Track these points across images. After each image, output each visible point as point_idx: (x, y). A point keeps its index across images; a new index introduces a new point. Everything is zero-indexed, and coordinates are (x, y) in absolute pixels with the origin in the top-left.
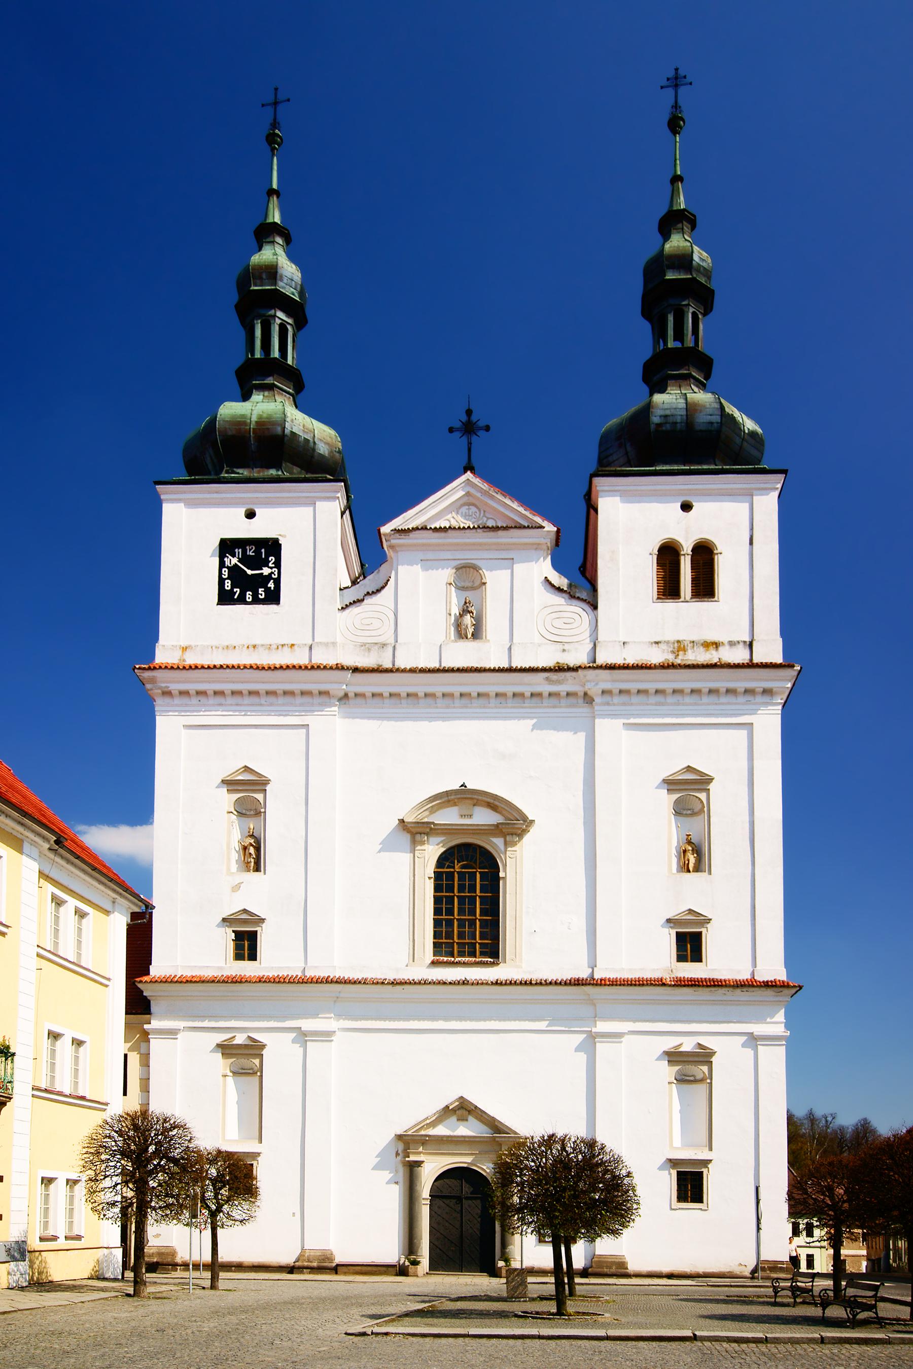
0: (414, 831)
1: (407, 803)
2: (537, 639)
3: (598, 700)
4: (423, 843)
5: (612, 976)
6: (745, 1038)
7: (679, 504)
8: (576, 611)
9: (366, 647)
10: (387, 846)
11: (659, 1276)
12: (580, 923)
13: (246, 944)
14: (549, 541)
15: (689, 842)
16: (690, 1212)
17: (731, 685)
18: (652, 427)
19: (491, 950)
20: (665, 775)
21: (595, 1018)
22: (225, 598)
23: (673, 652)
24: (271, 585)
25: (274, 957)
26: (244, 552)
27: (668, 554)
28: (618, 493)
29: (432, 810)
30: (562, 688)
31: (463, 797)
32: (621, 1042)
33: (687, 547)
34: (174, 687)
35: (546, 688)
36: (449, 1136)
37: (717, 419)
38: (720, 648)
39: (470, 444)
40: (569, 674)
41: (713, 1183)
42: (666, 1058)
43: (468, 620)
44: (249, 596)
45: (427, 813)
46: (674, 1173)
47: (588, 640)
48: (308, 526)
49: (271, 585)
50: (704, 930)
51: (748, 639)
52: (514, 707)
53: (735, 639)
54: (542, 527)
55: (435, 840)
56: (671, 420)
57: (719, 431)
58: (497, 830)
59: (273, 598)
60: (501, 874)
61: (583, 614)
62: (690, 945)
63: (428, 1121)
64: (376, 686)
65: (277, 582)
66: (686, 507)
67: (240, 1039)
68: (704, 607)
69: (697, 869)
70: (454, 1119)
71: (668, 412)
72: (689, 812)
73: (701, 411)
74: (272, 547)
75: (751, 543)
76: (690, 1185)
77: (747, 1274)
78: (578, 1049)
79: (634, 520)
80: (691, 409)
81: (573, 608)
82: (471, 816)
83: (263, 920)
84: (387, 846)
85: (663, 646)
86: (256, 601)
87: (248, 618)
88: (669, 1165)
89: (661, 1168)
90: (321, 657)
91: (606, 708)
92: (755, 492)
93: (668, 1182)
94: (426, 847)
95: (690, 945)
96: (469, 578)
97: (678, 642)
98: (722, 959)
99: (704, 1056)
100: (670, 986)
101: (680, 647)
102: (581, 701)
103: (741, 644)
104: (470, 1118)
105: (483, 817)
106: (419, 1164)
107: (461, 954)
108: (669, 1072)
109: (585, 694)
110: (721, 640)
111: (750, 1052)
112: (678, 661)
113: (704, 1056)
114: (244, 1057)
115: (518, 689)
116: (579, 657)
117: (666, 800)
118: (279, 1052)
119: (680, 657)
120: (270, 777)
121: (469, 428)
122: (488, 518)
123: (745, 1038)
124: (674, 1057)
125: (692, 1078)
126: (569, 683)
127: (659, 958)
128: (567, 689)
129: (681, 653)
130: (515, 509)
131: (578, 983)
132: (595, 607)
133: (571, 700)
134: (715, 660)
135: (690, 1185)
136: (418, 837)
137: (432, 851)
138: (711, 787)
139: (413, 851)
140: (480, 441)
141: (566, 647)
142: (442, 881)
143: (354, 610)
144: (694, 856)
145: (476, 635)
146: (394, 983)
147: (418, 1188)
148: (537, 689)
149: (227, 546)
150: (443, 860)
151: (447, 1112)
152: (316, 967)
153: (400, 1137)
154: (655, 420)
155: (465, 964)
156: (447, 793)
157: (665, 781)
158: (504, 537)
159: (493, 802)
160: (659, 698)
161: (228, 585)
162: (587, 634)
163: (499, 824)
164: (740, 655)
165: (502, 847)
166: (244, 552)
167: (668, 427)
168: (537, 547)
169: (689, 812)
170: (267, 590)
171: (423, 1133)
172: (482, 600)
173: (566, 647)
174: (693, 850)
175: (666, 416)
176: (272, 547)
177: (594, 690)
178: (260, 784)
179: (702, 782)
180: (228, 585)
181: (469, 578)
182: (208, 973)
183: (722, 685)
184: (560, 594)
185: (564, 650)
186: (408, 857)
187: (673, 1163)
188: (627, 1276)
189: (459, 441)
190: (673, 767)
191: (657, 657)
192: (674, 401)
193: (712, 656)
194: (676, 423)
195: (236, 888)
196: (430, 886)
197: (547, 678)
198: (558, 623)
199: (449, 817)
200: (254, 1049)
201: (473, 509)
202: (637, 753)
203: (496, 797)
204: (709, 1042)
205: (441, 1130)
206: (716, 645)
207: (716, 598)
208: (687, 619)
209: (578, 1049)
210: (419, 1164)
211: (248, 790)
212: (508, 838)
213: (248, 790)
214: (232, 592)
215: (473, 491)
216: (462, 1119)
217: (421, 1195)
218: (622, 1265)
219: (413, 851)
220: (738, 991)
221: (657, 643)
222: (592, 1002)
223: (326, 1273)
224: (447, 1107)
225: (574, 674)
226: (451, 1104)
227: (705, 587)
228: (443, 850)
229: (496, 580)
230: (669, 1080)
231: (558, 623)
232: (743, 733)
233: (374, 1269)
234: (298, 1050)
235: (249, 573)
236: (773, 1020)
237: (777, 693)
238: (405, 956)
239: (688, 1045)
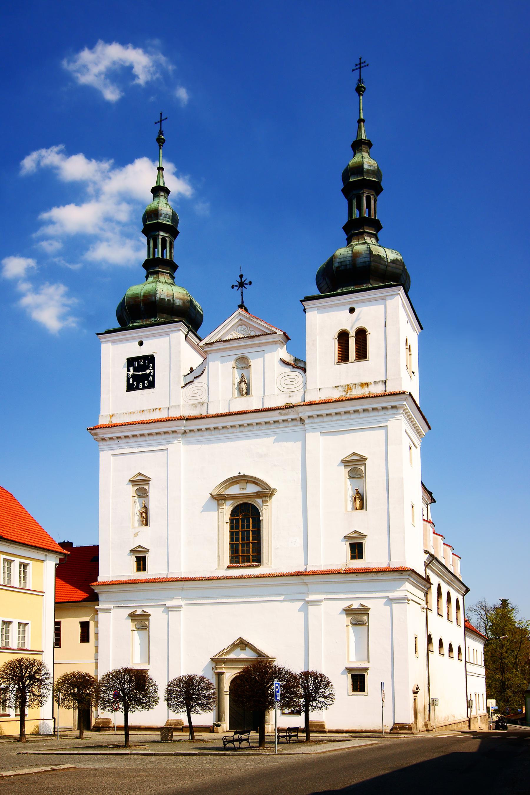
0: (219, 499)
2: (277, 392)
3: (307, 421)
4: (223, 505)
5: (315, 569)
6: (385, 600)
7: (348, 311)
8: (297, 374)
9: (195, 405)
10: (206, 508)
11: (342, 732)
12: (300, 541)
13: (141, 563)
14: (281, 339)
15: (358, 493)
16: (359, 696)
17: (374, 406)
18: (334, 269)
19: (257, 559)
20: (342, 458)
21: (308, 593)
22: (130, 388)
23: (345, 391)
24: (151, 379)
25: (154, 569)
26: (138, 363)
27: (343, 336)
28: (316, 308)
29: (226, 488)
30: (289, 417)
31: (241, 479)
32: (321, 605)
33: (352, 333)
34: (106, 436)
35: (281, 418)
36: (236, 658)
37: (367, 259)
38: (370, 386)
39: (242, 292)
40: (290, 410)
41: (370, 680)
42: (345, 612)
43: (243, 385)
44: (141, 386)
45: (223, 489)
46: (350, 676)
47: (302, 390)
48: (169, 346)
49: (151, 379)
50: (363, 541)
51: (384, 380)
52: (266, 429)
53: (377, 380)
54: (276, 333)
55: (229, 502)
56: (344, 264)
57: (369, 266)
58: (258, 495)
59: (152, 385)
60: (261, 518)
61: (300, 376)
62: (357, 550)
63: (225, 651)
64: (199, 425)
65: (153, 377)
66: (352, 310)
67: (139, 612)
68: (362, 364)
69: (362, 507)
70: (239, 649)
71: (342, 260)
72: (358, 476)
73: (359, 256)
74: (150, 359)
75: (385, 326)
76: (358, 682)
77: (388, 731)
78: (300, 610)
79: (325, 321)
80: (355, 255)
82: (245, 489)
83: (148, 550)
84: (206, 508)
85: (339, 388)
86: (144, 388)
87: (141, 396)
88: (347, 671)
89: (342, 673)
90: (174, 414)
91: (311, 425)
92: (387, 298)
93: (347, 680)
94: (224, 507)
95: (357, 550)
96: (243, 363)
97: (348, 385)
99: (365, 611)
100: (343, 573)
101: (348, 388)
102: (299, 422)
103: (381, 382)
104: (247, 648)
105: (252, 489)
106: (222, 673)
107: (243, 562)
108: (346, 620)
109: (301, 419)
110: (370, 381)
111: (389, 608)
112: (348, 396)
113: (365, 611)
114: (141, 621)
115: (267, 420)
116: (296, 399)
117: (344, 472)
118: (157, 617)
119: (348, 393)
121: (241, 285)
122: (251, 331)
123: (385, 600)
124: (348, 611)
125: (361, 623)
126: (291, 415)
128: (290, 417)
129: (349, 391)
130: (263, 325)
131: (298, 574)
132: (305, 370)
133: (294, 423)
134: (367, 394)
135: (358, 682)
136: (220, 502)
137: (227, 509)
138: (366, 462)
139: (218, 510)
140: (247, 291)
142: (234, 524)
143: (189, 387)
145: (248, 393)
146: (208, 579)
147: (222, 686)
148: (276, 419)
149: (130, 362)
150: (234, 513)
151: (234, 646)
152: (172, 573)
153: (212, 659)
154: (336, 265)
155: (244, 567)
156: (232, 478)
157: (342, 461)
158: (257, 341)
159: (255, 481)
160: (338, 417)
161: (131, 381)
162: (302, 386)
163: (257, 492)
164: (379, 389)
165: (261, 503)
166: (138, 363)
167: (343, 268)
168: (276, 342)
169: (358, 476)
170: (149, 382)
171: (224, 657)
172: (249, 374)
173: (291, 394)
174: (359, 497)
175: (341, 262)
176: (150, 359)
177: (304, 415)
178: (147, 481)
179: (362, 460)
180: (131, 381)
181: (243, 363)
182: (124, 579)
183: (370, 407)
184: (288, 366)
185: (290, 396)
186: (216, 513)
187: (349, 670)
188: (325, 732)
189: (236, 292)
190: (345, 454)
191: (336, 395)
192: (346, 253)
193: (365, 391)
194: (347, 265)
195: (136, 535)
196: (227, 528)
197: (280, 413)
198: (287, 382)
199: (235, 490)
200: (146, 616)
201: (244, 327)
202: (327, 448)
203: (255, 478)
204: (366, 603)
205: (232, 656)
206: (367, 384)
207: (367, 359)
208: (354, 372)
209: (300, 610)
210: (222, 673)
211: (141, 485)
212: (264, 499)
213: (141, 485)
214: (133, 384)
215: (242, 318)
216: (243, 649)
217: (223, 690)
218: (322, 726)
219: (218, 510)
220: (379, 574)
221: (336, 387)
222: (306, 584)
223: (178, 731)
224: (234, 643)
225: (292, 409)
226: (236, 641)
227: (362, 354)
228: (232, 508)
229: (256, 363)
230: (346, 624)
231: (287, 382)
232: (383, 432)
233: (200, 729)
234: (165, 616)
235: (141, 373)
236: (401, 589)
237: (399, 408)
238: (215, 565)
239: (356, 605)
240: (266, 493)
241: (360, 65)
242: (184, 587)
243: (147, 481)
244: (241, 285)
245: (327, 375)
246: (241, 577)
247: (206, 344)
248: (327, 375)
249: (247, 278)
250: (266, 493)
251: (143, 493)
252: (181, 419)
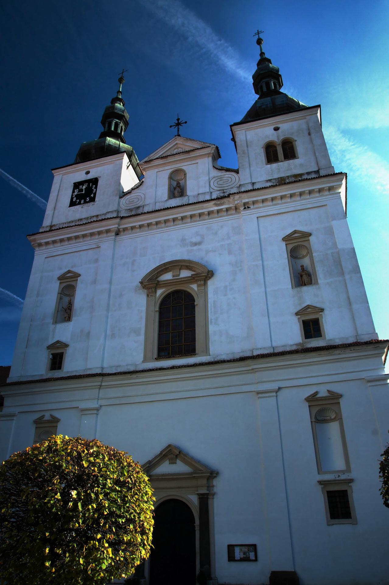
16: (342, 529)
24: (92, 195)
25: (71, 365)
39: (178, 129)
49: (92, 195)
58: (192, 279)
60: (195, 304)
81: (227, 176)
86: (85, 202)
120: (80, 272)
121: (178, 124)
141: (225, 191)
158: (193, 154)
161: (74, 199)
167: (264, 107)
198: (221, 182)
203: (189, 261)
214: (76, 201)
216: (173, 462)
231: (221, 182)
241: (258, 33)
242: (103, 384)
243: (77, 276)
244: (178, 124)
246: (173, 368)
247: (146, 162)
249: (182, 120)
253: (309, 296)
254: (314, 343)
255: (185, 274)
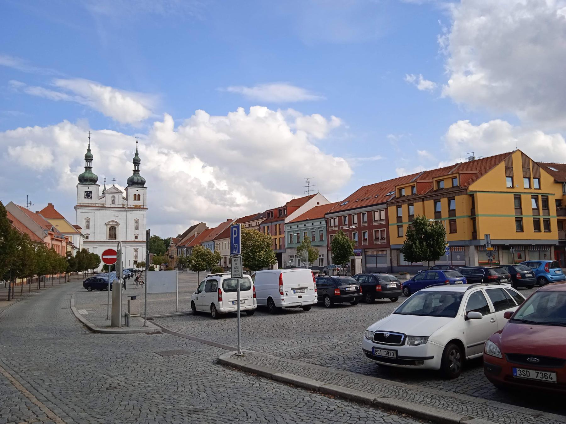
1: (106, 222)
22: (85, 198)
25: (90, 239)
59: (91, 198)
62: (136, 237)
74: (91, 192)
95: (136, 237)
98: (140, 239)
99: (138, 249)
105: (114, 224)
127: (133, 238)
131: (124, 241)
142: (110, 230)
144: (137, 228)
149: (86, 192)
176: (91, 192)
189: (113, 182)
199: (111, 223)
208: (137, 203)
240: (118, 224)
243: (90, 219)
245: (132, 202)
248: (132, 202)
250: (118, 224)
251: (88, 222)
252: (99, 207)
253: (137, 232)
254: (136, 240)
255: (114, 224)
